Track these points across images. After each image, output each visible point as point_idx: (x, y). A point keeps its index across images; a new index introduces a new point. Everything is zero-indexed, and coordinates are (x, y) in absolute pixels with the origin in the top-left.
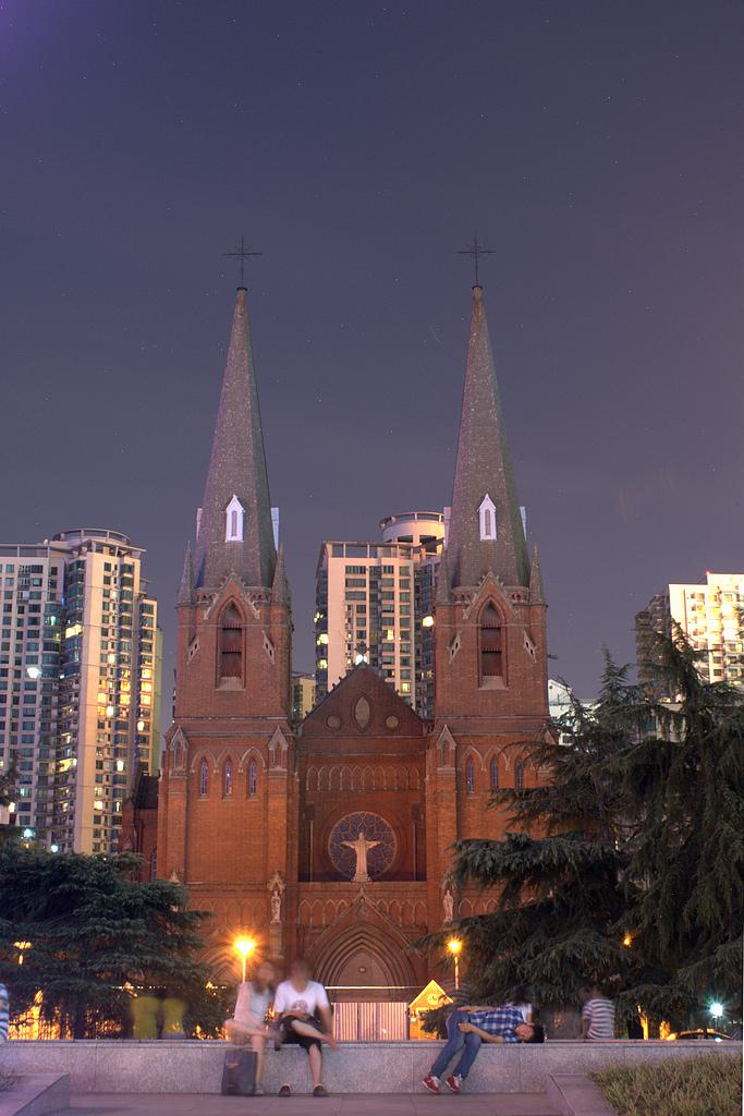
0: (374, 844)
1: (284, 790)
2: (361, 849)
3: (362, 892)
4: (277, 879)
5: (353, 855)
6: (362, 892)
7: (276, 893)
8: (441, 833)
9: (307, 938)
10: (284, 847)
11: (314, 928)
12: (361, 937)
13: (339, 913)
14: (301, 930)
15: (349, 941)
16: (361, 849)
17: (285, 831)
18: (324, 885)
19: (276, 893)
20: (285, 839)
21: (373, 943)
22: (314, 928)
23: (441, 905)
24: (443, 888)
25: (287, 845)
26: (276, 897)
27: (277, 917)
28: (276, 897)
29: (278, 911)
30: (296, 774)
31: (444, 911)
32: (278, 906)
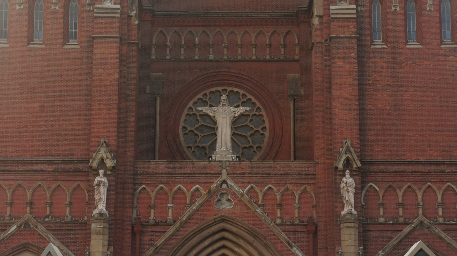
0: (241, 110)
1: (115, 33)
2: (224, 116)
3: (224, 176)
4: (103, 153)
5: (211, 127)
6: (224, 176)
7: (101, 172)
8: (335, 93)
9: (146, 238)
10: (115, 111)
11: (157, 224)
12: (223, 238)
13: (192, 203)
14: (138, 229)
15: (206, 243)
16: (224, 116)
17: (116, 89)
18: (171, 166)
19: (101, 172)
20: (115, 98)
21: (239, 246)
22: (157, 224)
23: (338, 190)
24: (341, 165)
25: (119, 110)
26: (101, 178)
27: (101, 207)
28: (101, 178)
29: (104, 197)
30: (133, 13)
31: (341, 198)
32: (103, 190)
